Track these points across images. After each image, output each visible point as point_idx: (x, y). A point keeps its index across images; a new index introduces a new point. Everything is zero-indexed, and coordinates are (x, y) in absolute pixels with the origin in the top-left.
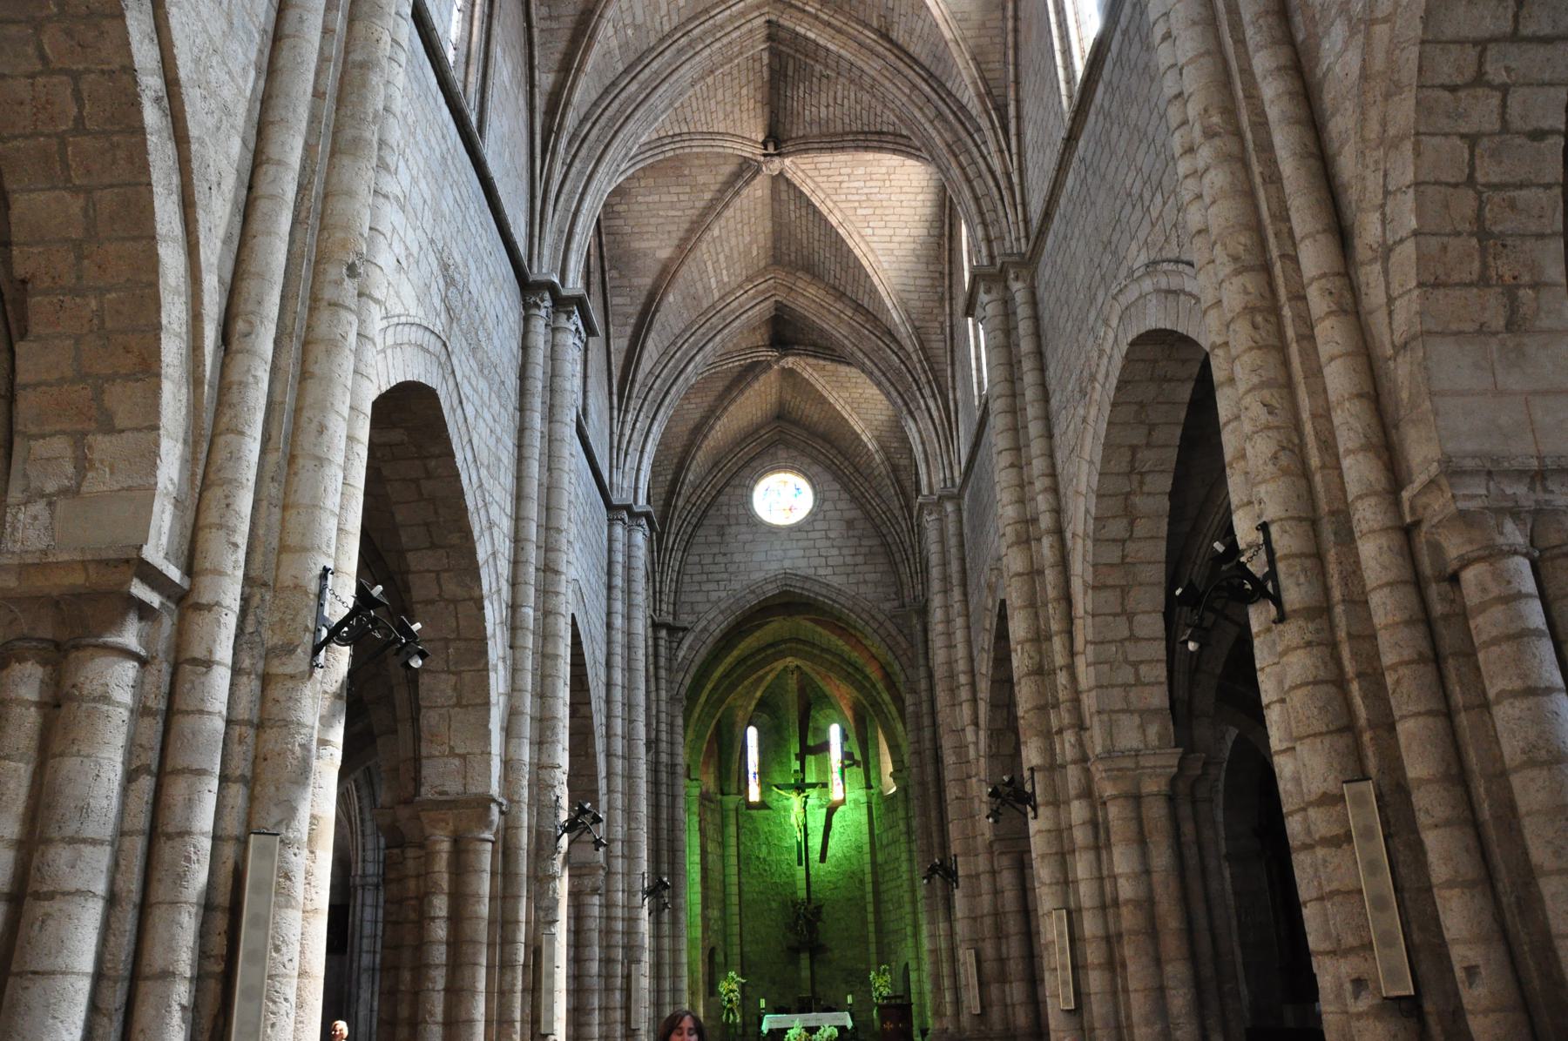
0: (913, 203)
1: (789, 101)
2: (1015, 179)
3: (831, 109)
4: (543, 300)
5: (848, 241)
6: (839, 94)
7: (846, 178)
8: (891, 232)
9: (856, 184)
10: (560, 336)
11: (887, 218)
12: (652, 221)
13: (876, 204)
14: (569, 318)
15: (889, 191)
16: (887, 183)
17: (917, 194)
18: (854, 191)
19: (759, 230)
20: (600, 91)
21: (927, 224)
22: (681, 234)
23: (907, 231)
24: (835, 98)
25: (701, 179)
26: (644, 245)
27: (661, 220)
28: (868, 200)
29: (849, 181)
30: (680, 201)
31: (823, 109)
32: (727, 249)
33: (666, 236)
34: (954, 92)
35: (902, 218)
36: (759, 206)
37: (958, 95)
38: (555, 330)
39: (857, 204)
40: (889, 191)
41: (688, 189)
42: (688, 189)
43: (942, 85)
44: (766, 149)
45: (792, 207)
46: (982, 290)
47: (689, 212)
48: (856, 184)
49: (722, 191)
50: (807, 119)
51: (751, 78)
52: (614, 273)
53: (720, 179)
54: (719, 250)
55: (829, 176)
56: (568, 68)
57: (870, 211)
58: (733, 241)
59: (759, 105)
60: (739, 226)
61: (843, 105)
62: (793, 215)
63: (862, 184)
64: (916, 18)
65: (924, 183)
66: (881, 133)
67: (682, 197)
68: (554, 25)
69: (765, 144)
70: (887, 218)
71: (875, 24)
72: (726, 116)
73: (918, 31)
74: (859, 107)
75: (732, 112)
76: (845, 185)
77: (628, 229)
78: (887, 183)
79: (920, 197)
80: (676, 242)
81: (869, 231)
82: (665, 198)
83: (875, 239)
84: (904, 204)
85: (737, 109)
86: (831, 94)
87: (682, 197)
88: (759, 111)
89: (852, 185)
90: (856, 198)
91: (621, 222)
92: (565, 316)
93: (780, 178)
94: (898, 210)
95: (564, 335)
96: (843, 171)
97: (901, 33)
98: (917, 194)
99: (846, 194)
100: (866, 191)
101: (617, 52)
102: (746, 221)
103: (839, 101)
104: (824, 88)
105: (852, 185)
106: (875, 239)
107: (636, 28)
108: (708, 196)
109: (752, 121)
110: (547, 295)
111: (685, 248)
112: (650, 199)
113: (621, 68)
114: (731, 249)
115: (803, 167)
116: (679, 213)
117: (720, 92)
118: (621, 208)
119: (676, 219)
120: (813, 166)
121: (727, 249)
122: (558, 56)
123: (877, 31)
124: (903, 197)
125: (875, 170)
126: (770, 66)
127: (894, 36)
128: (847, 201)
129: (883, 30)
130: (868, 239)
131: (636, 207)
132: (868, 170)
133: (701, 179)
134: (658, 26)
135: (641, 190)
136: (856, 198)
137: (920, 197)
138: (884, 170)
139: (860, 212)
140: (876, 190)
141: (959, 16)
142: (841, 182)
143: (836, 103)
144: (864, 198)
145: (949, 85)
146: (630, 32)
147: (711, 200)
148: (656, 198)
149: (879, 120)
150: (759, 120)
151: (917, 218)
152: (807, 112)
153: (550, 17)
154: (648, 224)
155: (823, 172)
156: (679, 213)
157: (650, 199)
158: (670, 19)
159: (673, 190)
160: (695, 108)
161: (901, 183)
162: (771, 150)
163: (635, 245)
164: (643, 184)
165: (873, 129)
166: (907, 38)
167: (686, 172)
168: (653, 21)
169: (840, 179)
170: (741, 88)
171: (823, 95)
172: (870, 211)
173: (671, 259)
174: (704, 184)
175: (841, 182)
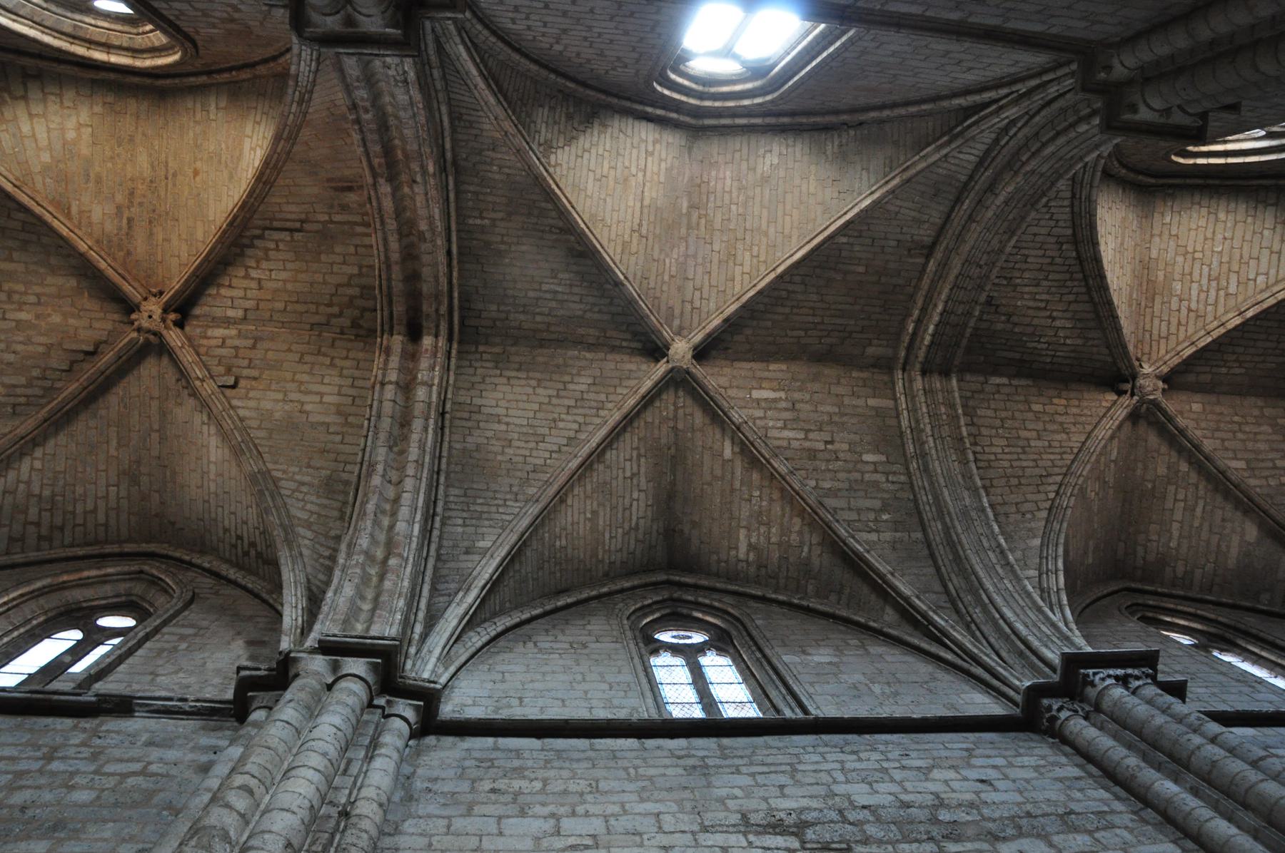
0: (1229, 225)
1: (1059, 360)
2: (1022, 88)
3: (1055, 314)
4: (1049, 708)
5: (1265, 305)
6: (1031, 304)
7: (1185, 303)
8: (1266, 252)
9: (1194, 293)
10: (1106, 703)
11: (1246, 256)
12: (1204, 535)
13: (1225, 267)
14: (1093, 684)
15: (1208, 253)
16: (1198, 255)
17: (1217, 220)
18: (1203, 296)
19: (1256, 412)
20: (931, 562)
21: (1260, 207)
22: (1229, 507)
23: (1266, 233)
24: (1039, 309)
25: (1162, 470)
26: (1234, 552)
27: (1206, 527)
28: (1217, 279)
29: (1189, 300)
30: (1185, 500)
31: (1058, 323)
32: (1271, 456)
33: (1229, 525)
34: (969, 172)
35: (1248, 237)
36: (1218, 409)
37: (971, 167)
38: (1098, 708)
39: (1222, 293)
40: (1208, 253)
41: (1172, 488)
42: (1172, 488)
43: (966, 184)
44: (1125, 392)
45: (1224, 370)
46: (1127, 117)
47: (1201, 493)
48: (1194, 293)
49: (1181, 450)
50: (1079, 342)
51: (1022, 398)
52: (1265, 597)
53: (1164, 449)
54: (1270, 465)
55: (1179, 324)
56: (884, 592)
57: (1234, 278)
58: (1262, 446)
59: (1064, 394)
60: (1240, 435)
61: (1047, 301)
62: (1237, 371)
63: (1195, 286)
64: (900, 216)
65: (1204, 211)
66: (1079, 257)
67: (1181, 496)
68: (847, 591)
69: (1120, 393)
70: (1246, 256)
71: (921, 260)
72: (1064, 431)
73: (913, 214)
74: (1045, 283)
75: (1061, 424)
76: (1194, 306)
77: (1209, 567)
78: (1198, 255)
79: (1222, 216)
80: (1239, 514)
81: (1261, 279)
82: (1178, 515)
83: (1273, 272)
84: (1228, 235)
85: (1060, 419)
86: (1031, 312)
87: (1181, 496)
88: (1072, 395)
89: (1194, 298)
90: (1213, 293)
91: (1198, 572)
92: (1089, 689)
93: (1172, 380)
94: (1236, 244)
95: (1106, 699)
96: (1174, 306)
97: (922, 232)
98: (1217, 220)
99: (1206, 304)
100: (1204, 281)
101: (898, 535)
102: (1236, 427)
103: (1043, 305)
104: (1027, 320)
105: (1194, 298)
106: (1273, 272)
107: (884, 509)
108: (1184, 467)
109: (1085, 404)
110: (1045, 702)
111: (1247, 505)
112: (1176, 534)
113: (919, 535)
114: (1272, 450)
115: (1162, 352)
116: (1201, 503)
117: (1023, 434)
118: (1180, 570)
119: (1208, 508)
120: (1163, 342)
121: (1271, 456)
122: (873, 597)
123: (928, 257)
124: (1219, 237)
125: (1178, 269)
126: (1010, 377)
127: (928, 240)
128: (1216, 304)
129: (925, 252)
130: (1272, 280)
131: (1184, 549)
132: (1177, 277)
133: (1162, 470)
134: (897, 487)
135: (1162, 540)
136: (1213, 293)
137: (1222, 216)
138: (1180, 259)
139: (1232, 289)
140: (1206, 269)
141: (887, 169)
142: (1190, 310)
143: (1045, 309)
144: (1214, 284)
145: (963, 178)
146: (885, 517)
147: (1190, 463)
148: (1175, 526)
149: (1058, 260)
150: (1086, 395)
151: (1250, 220)
152: (1068, 341)
153: (840, 593)
154: (1208, 542)
155: (1173, 330)
156: (1201, 503)
157: (1176, 534)
158: (894, 473)
159: (1169, 505)
160: (1031, 464)
161: (1201, 237)
162: (1128, 386)
163: (1231, 563)
164: (1155, 537)
165: (1077, 268)
166: (926, 226)
167: (1150, 486)
168: (887, 492)
169: (1184, 311)
170: (1030, 410)
171: (1036, 322)
172: (1234, 278)
173: (1261, 526)
174: (1168, 468)
175: (1190, 310)
